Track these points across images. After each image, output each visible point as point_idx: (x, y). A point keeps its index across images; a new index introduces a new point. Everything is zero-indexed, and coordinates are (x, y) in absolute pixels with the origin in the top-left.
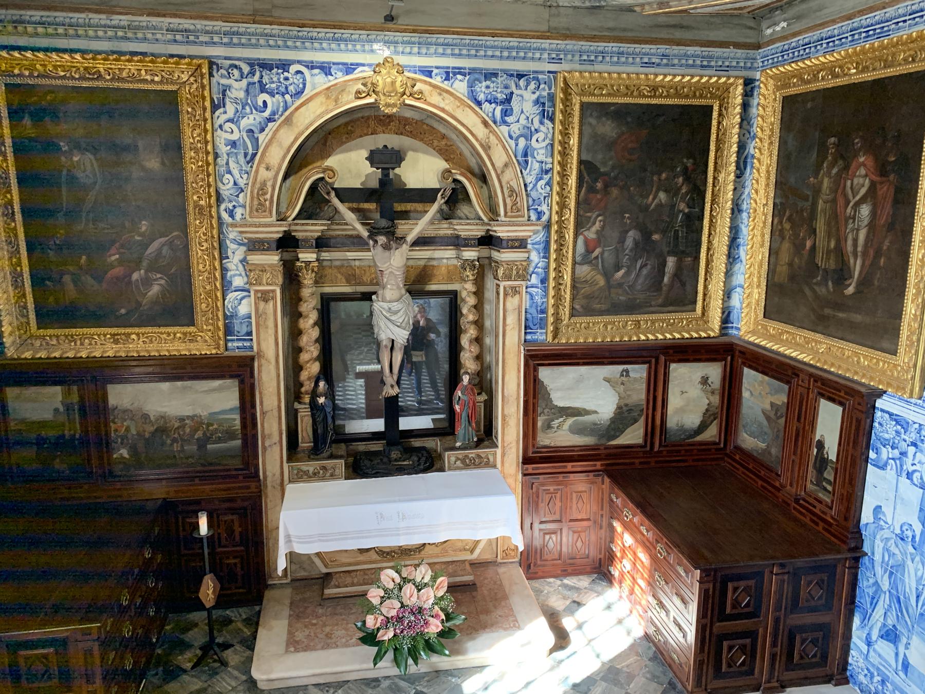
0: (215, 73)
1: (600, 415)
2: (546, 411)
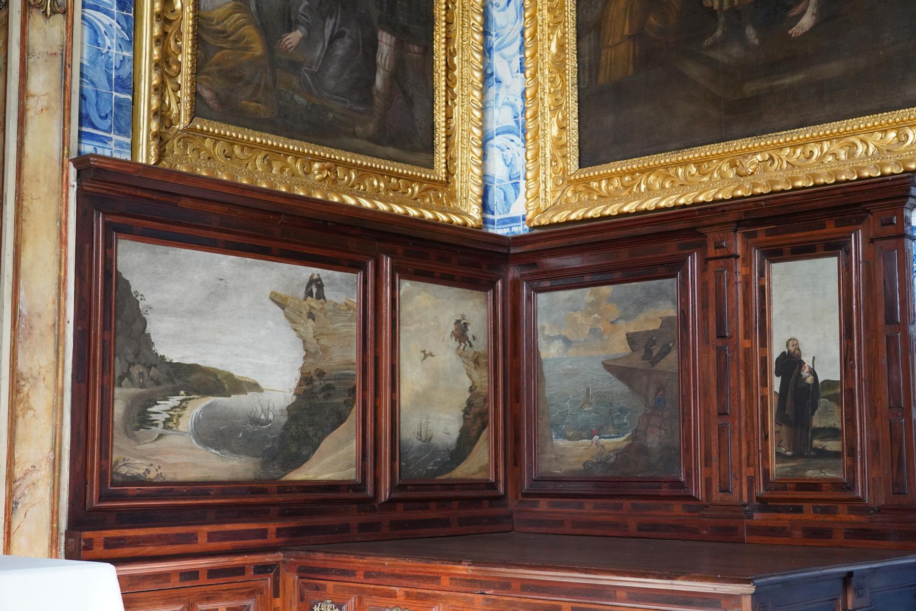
1: (265, 396)
2: (136, 371)
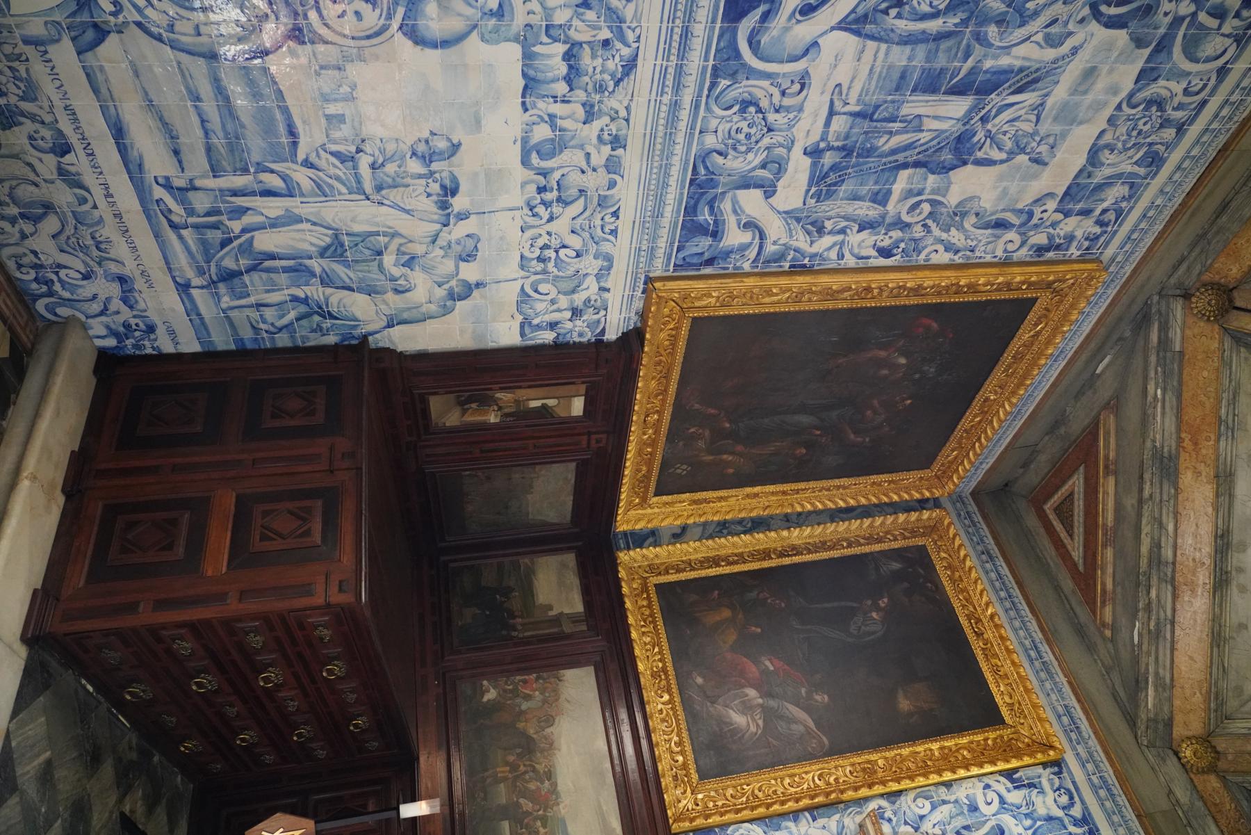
0: (1049, 770)
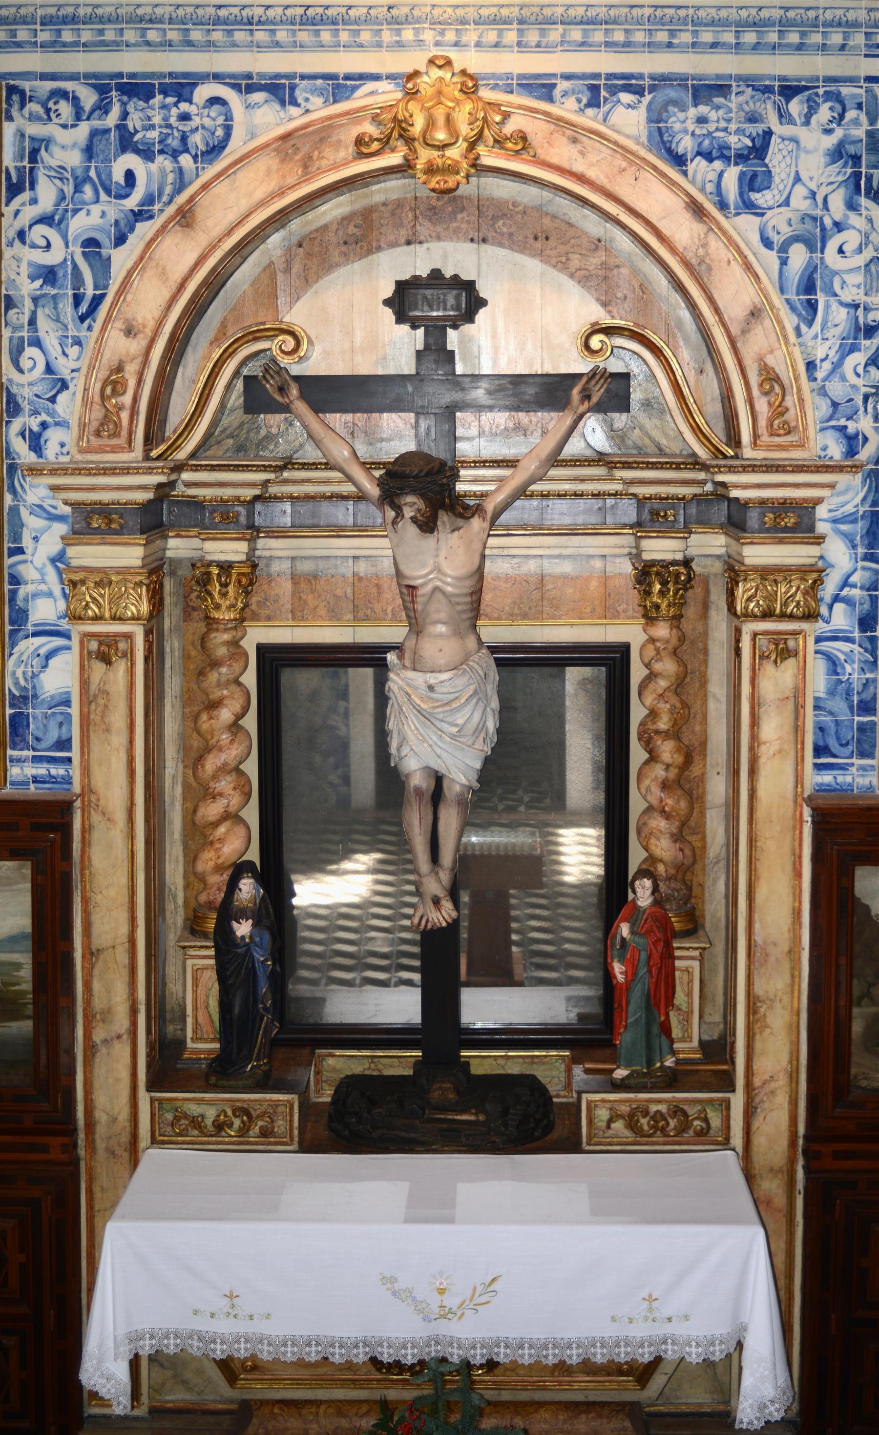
0: (15, 113)
